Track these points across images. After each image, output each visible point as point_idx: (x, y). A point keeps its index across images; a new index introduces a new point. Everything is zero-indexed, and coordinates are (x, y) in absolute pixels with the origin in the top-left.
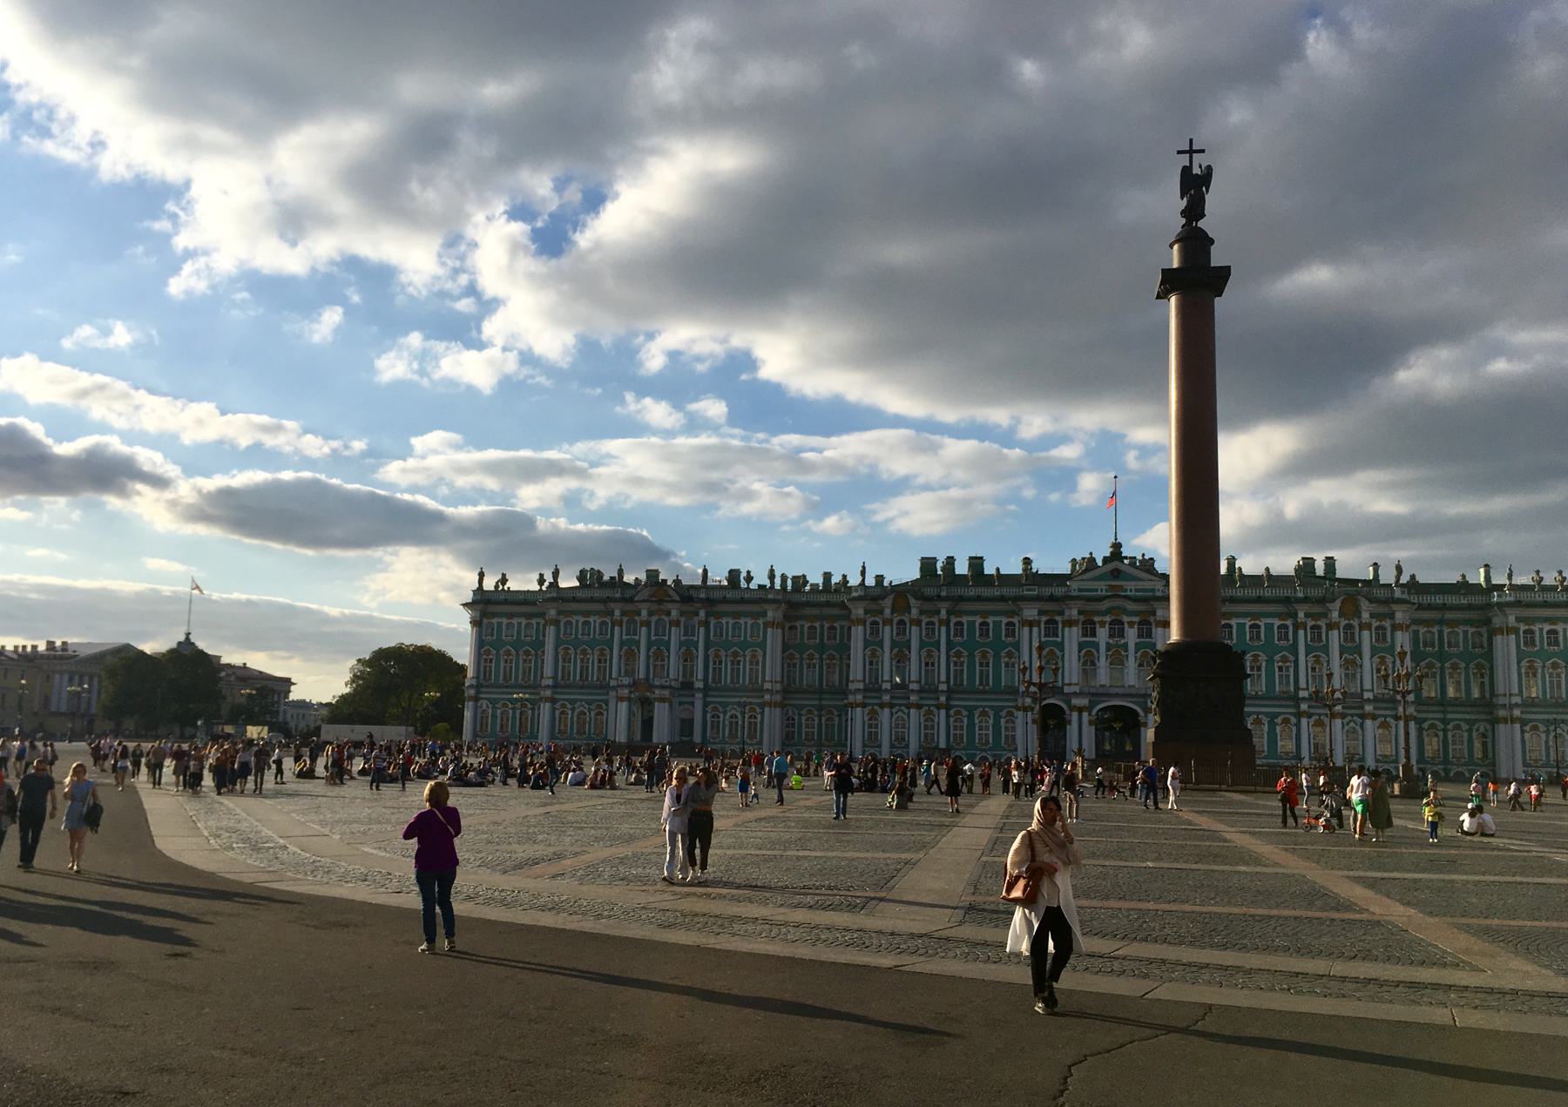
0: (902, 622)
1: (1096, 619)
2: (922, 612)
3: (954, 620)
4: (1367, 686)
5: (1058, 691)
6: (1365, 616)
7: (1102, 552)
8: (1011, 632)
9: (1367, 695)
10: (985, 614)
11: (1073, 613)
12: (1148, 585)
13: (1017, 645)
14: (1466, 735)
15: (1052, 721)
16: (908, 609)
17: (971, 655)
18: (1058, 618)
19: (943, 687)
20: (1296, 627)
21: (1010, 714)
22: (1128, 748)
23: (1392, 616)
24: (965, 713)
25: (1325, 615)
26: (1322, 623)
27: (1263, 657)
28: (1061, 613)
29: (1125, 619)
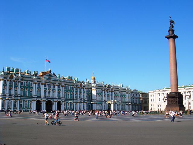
0: (11, 81)
1: (47, 84)
2: (15, 79)
3: (21, 81)
5: (40, 97)
9: (83, 99)
12: (55, 78)
13: (33, 88)
15: (39, 104)
17: (24, 90)
18: (40, 83)
20: (74, 87)
21: (31, 102)
22: (50, 108)
24: (23, 101)
26: (77, 87)
27: (70, 92)
28: (41, 82)
29: (51, 84)
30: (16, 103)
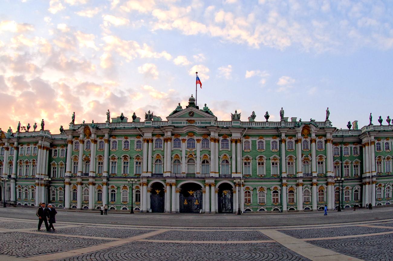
1: (181, 138)
3: (112, 140)
4: (314, 170)
6: (313, 135)
7: (185, 105)
8: (139, 146)
10: (126, 137)
11: (168, 134)
14: (350, 191)
16: (90, 135)
18: (162, 138)
19: (105, 174)
20: (281, 141)
23: (325, 136)
25: (295, 136)
26: (293, 140)
28: (163, 135)
30: (101, 191)
